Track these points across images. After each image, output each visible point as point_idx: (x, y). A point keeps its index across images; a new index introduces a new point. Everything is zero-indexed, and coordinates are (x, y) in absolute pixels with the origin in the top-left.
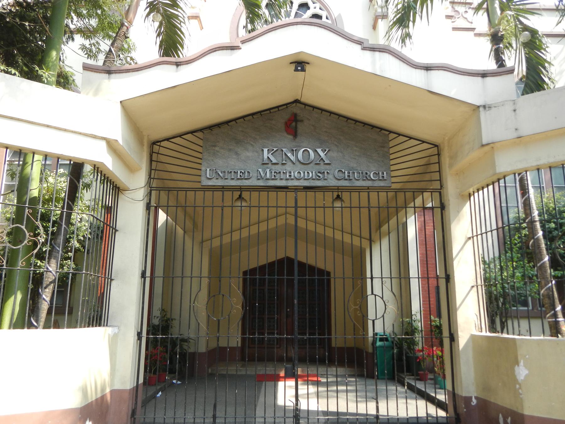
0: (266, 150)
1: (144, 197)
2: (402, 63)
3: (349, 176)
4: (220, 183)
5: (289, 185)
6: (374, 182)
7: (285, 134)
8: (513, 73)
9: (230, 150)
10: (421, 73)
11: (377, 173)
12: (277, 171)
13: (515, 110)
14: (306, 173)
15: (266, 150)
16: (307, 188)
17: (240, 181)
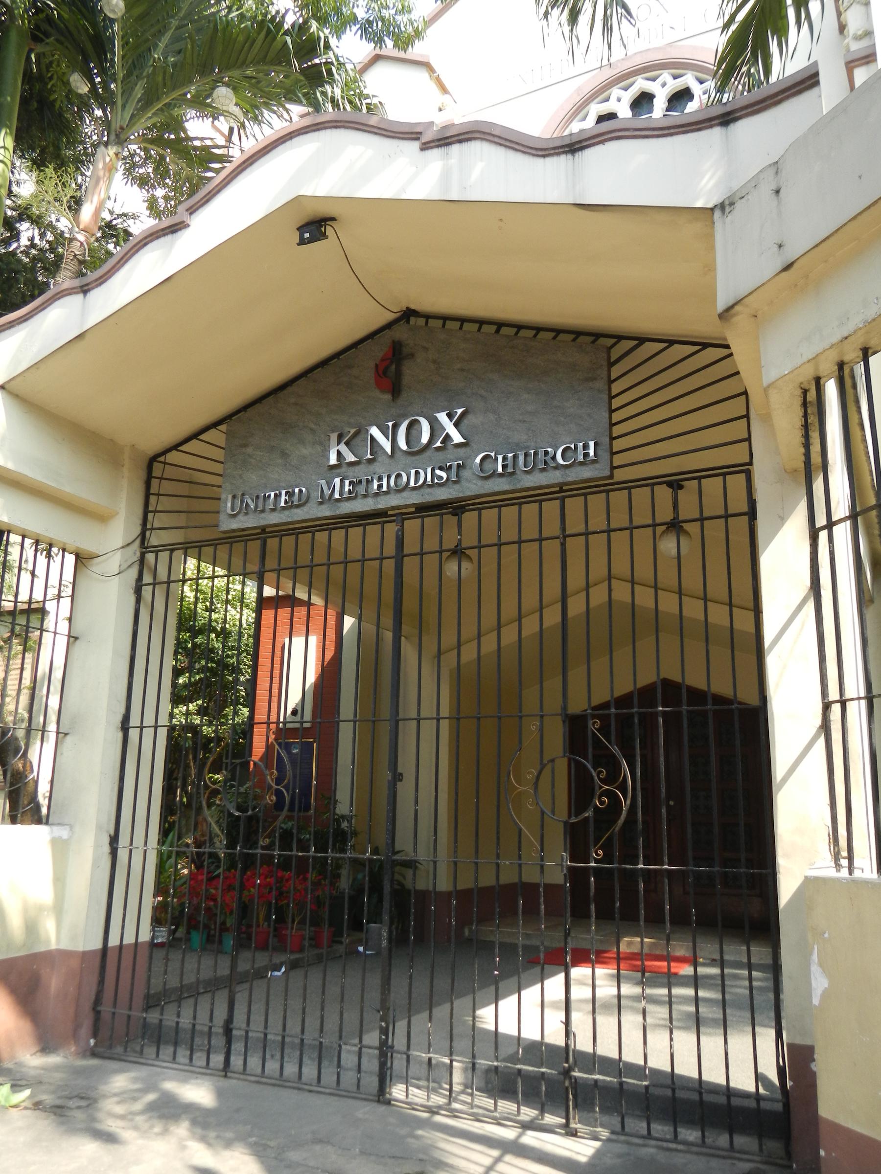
0: (334, 437)
1: (125, 566)
2: (511, 154)
3: (505, 467)
5: (380, 506)
6: (567, 471)
7: (377, 393)
8: (817, 83)
9: (272, 449)
11: (572, 446)
12: (355, 480)
13: (777, 192)
16: (423, 509)
17: (287, 512)
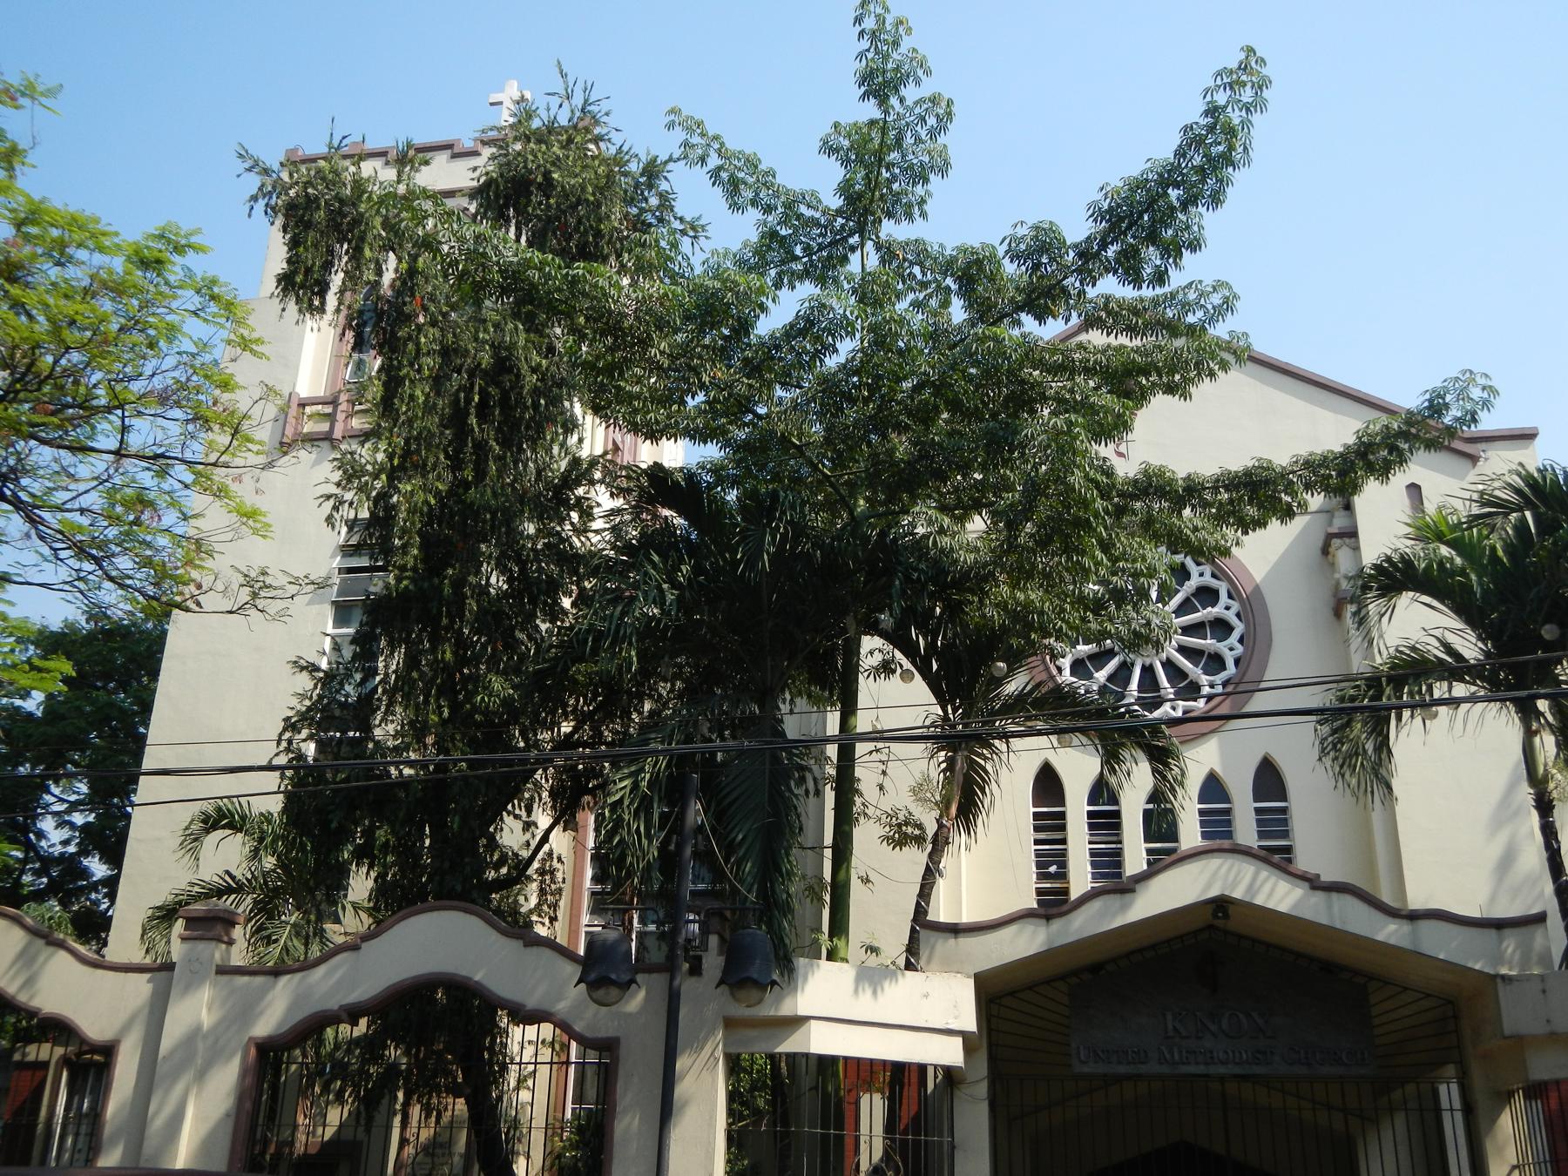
0: (1169, 1017)
4: (1101, 1069)
13: (1544, 991)
14: (1237, 1055)
15: (1169, 1017)
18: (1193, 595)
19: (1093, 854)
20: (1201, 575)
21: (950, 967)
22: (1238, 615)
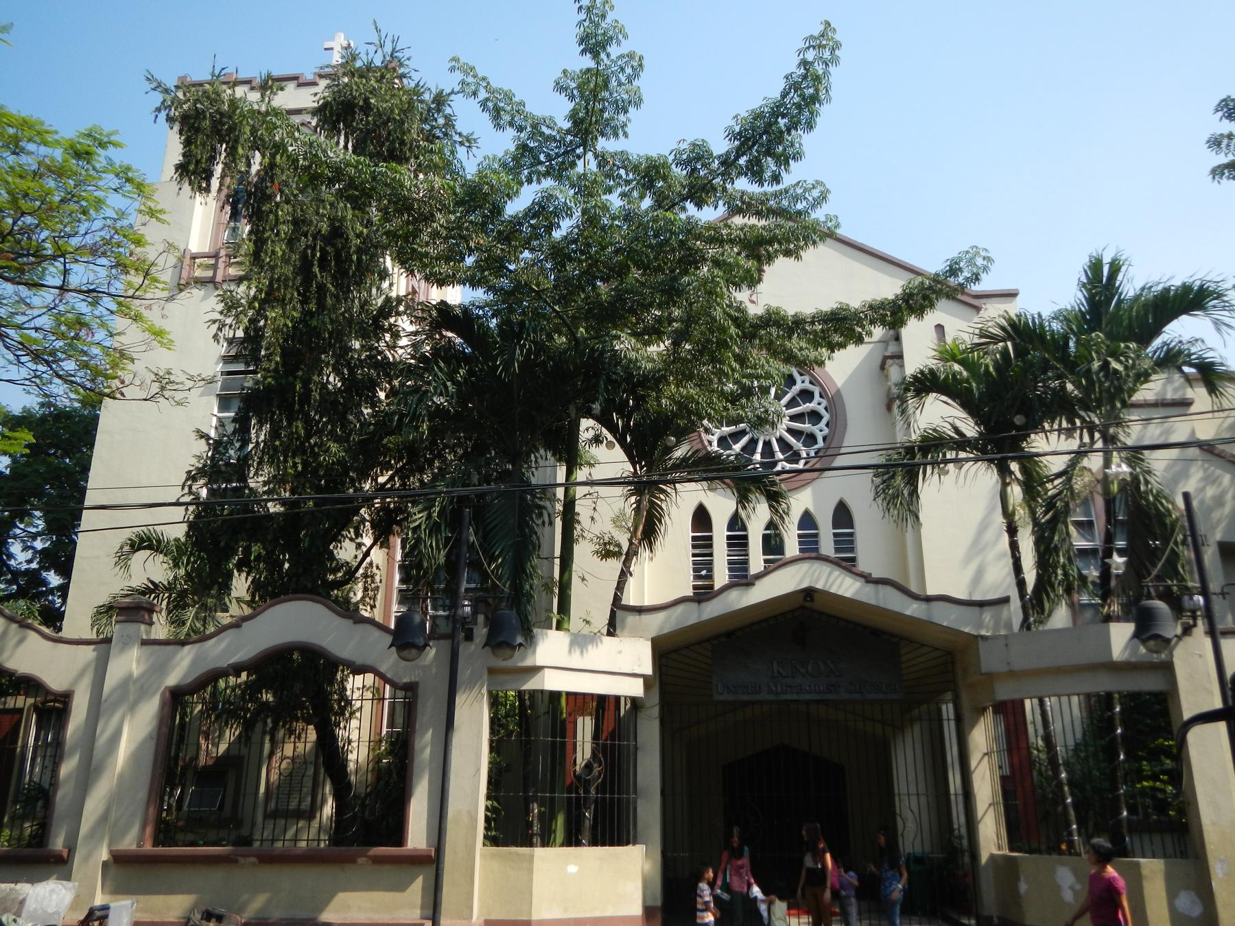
4: (731, 697)
10: (924, 606)
13: (1007, 645)
16: (818, 702)
18: (798, 395)
19: (730, 563)
20: (803, 382)
21: (636, 633)
22: (826, 409)
